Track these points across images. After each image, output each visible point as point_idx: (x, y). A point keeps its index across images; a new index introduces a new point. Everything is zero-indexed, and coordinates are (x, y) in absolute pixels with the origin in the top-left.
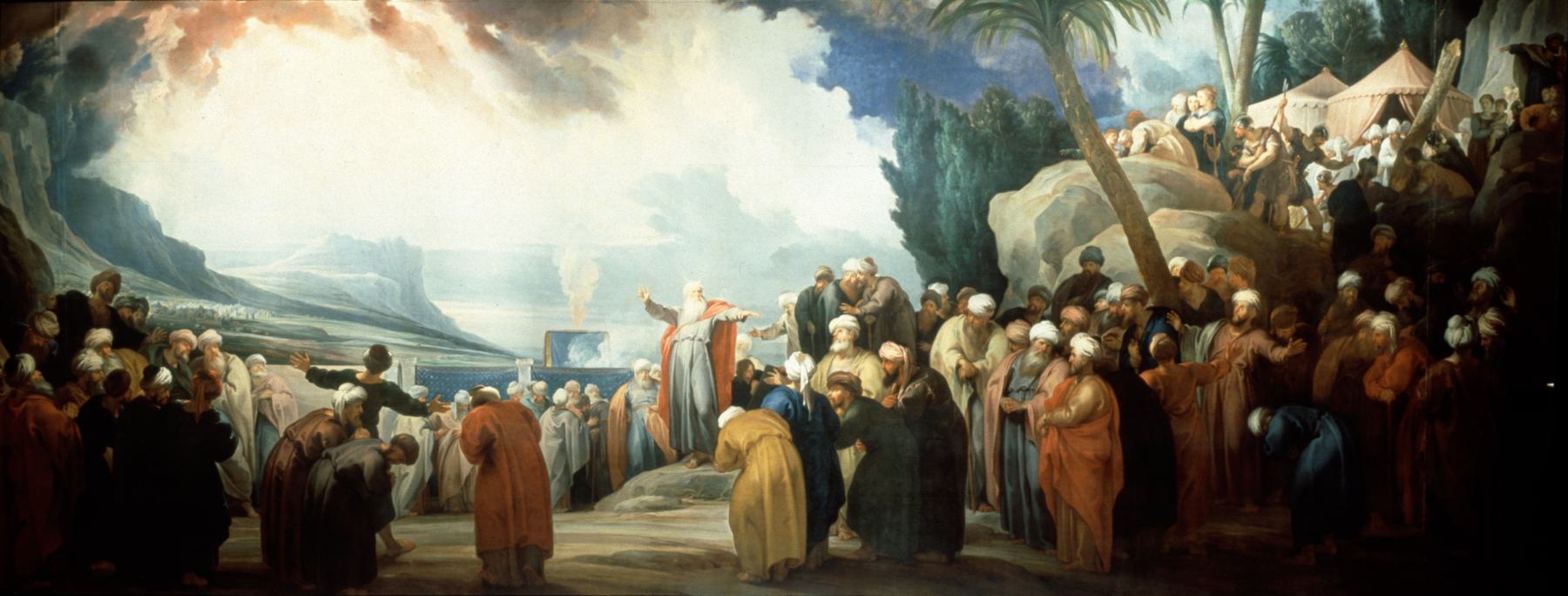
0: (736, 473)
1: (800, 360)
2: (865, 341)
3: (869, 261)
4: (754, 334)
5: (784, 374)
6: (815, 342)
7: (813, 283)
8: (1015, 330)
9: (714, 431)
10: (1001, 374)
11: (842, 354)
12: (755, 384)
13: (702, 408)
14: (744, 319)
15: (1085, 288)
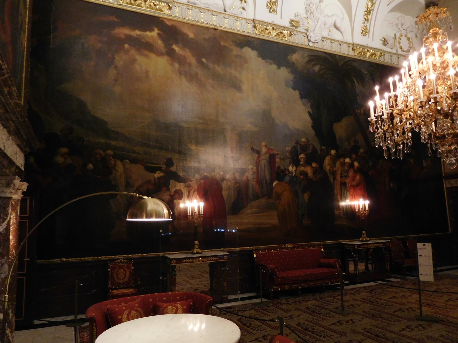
0: (278, 201)
1: (293, 167)
2: (308, 162)
3: (307, 139)
4: (280, 159)
5: (288, 170)
6: (296, 162)
8: (342, 160)
10: (339, 172)
12: (282, 174)
14: (278, 154)
15: (355, 149)
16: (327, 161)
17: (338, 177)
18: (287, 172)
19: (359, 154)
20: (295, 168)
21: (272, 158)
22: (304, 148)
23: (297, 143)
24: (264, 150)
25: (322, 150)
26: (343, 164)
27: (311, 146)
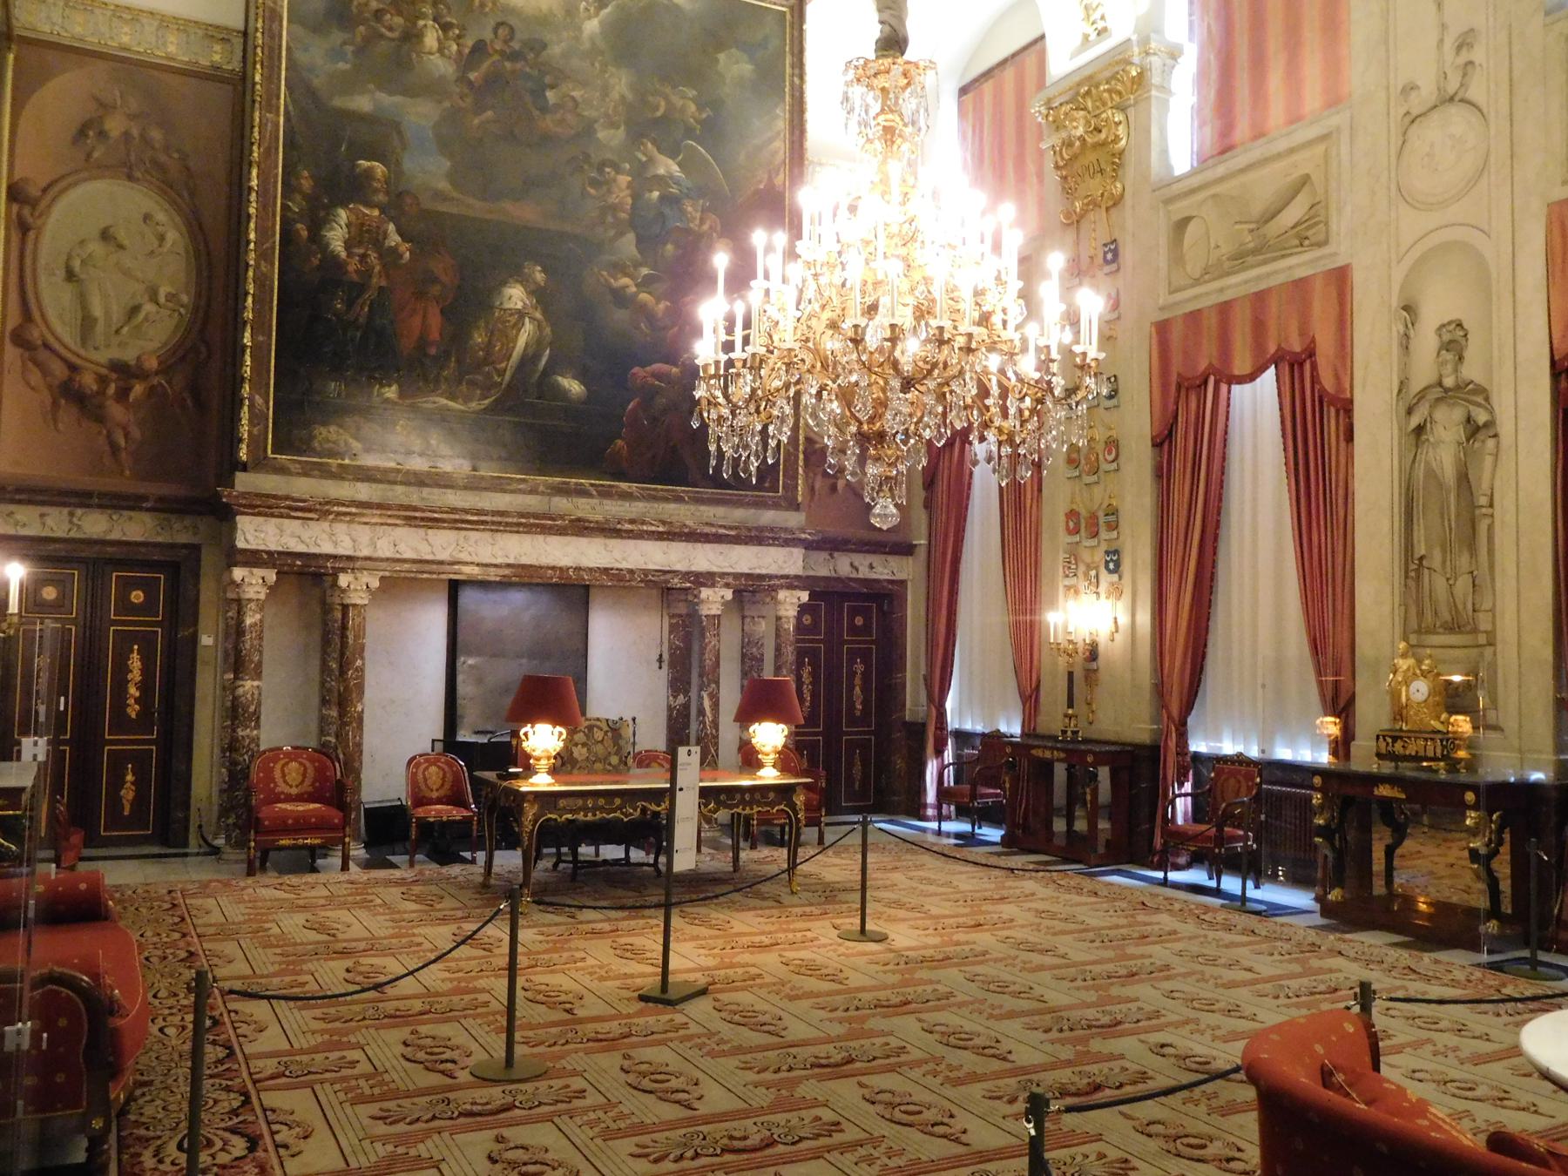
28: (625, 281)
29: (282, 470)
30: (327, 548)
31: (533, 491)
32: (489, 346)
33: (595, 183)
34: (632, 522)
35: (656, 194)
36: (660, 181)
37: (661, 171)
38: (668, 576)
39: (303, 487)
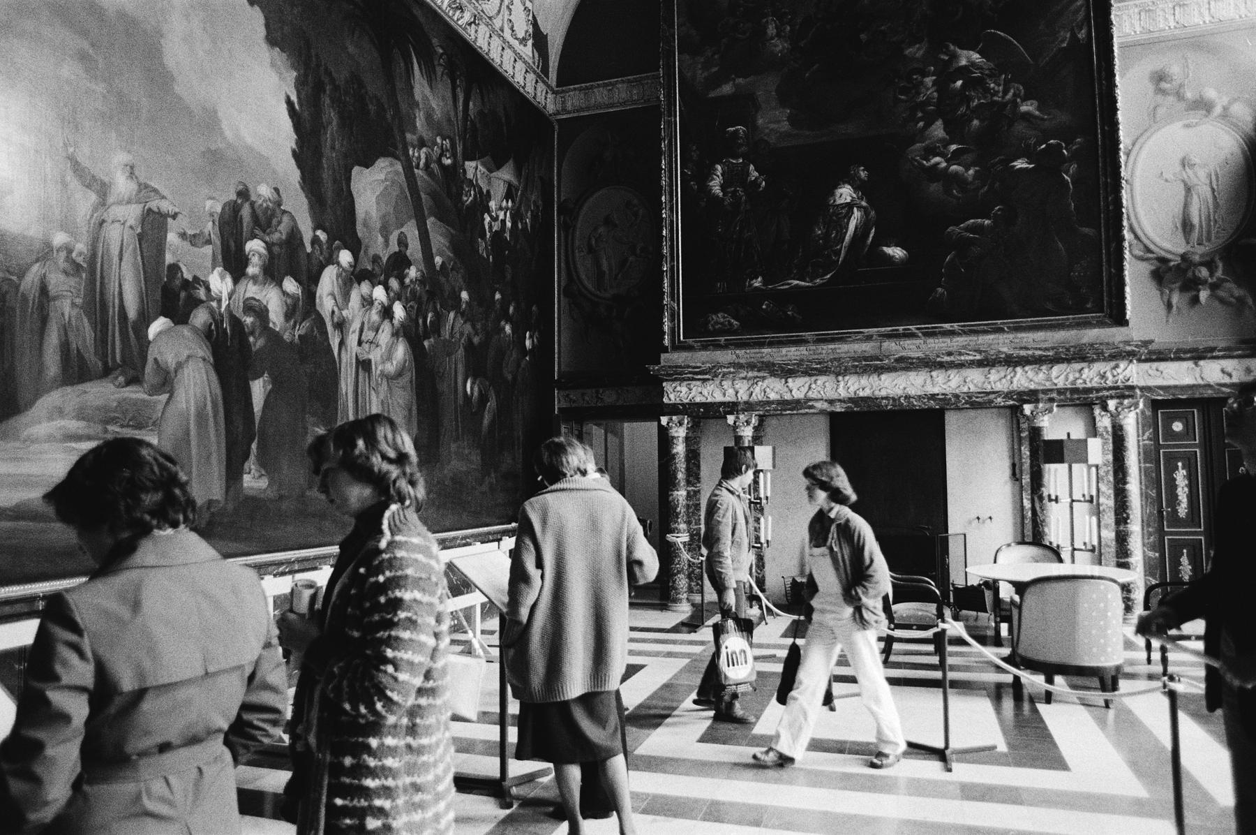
0: (164, 397)
1: (222, 278)
2: (272, 274)
3: (277, 190)
4: (183, 235)
5: (208, 289)
6: (235, 264)
7: (234, 197)
8: (365, 287)
9: (144, 343)
10: (356, 326)
11: (254, 278)
12: (183, 294)
13: (132, 313)
14: (174, 216)
15: (399, 263)
16: (328, 280)
17: (352, 339)
18: (202, 293)
19: (407, 281)
20: (229, 280)
21: (153, 226)
22: (264, 221)
23: (244, 194)
24: (122, 185)
25: (315, 241)
26: (368, 302)
27: (285, 219)
28: (937, 159)
29: (690, 348)
30: (719, 398)
31: (869, 338)
32: (827, 235)
33: (904, 91)
34: (950, 354)
35: (959, 83)
36: (964, 72)
37: (963, 62)
38: (992, 396)
39: (701, 358)
